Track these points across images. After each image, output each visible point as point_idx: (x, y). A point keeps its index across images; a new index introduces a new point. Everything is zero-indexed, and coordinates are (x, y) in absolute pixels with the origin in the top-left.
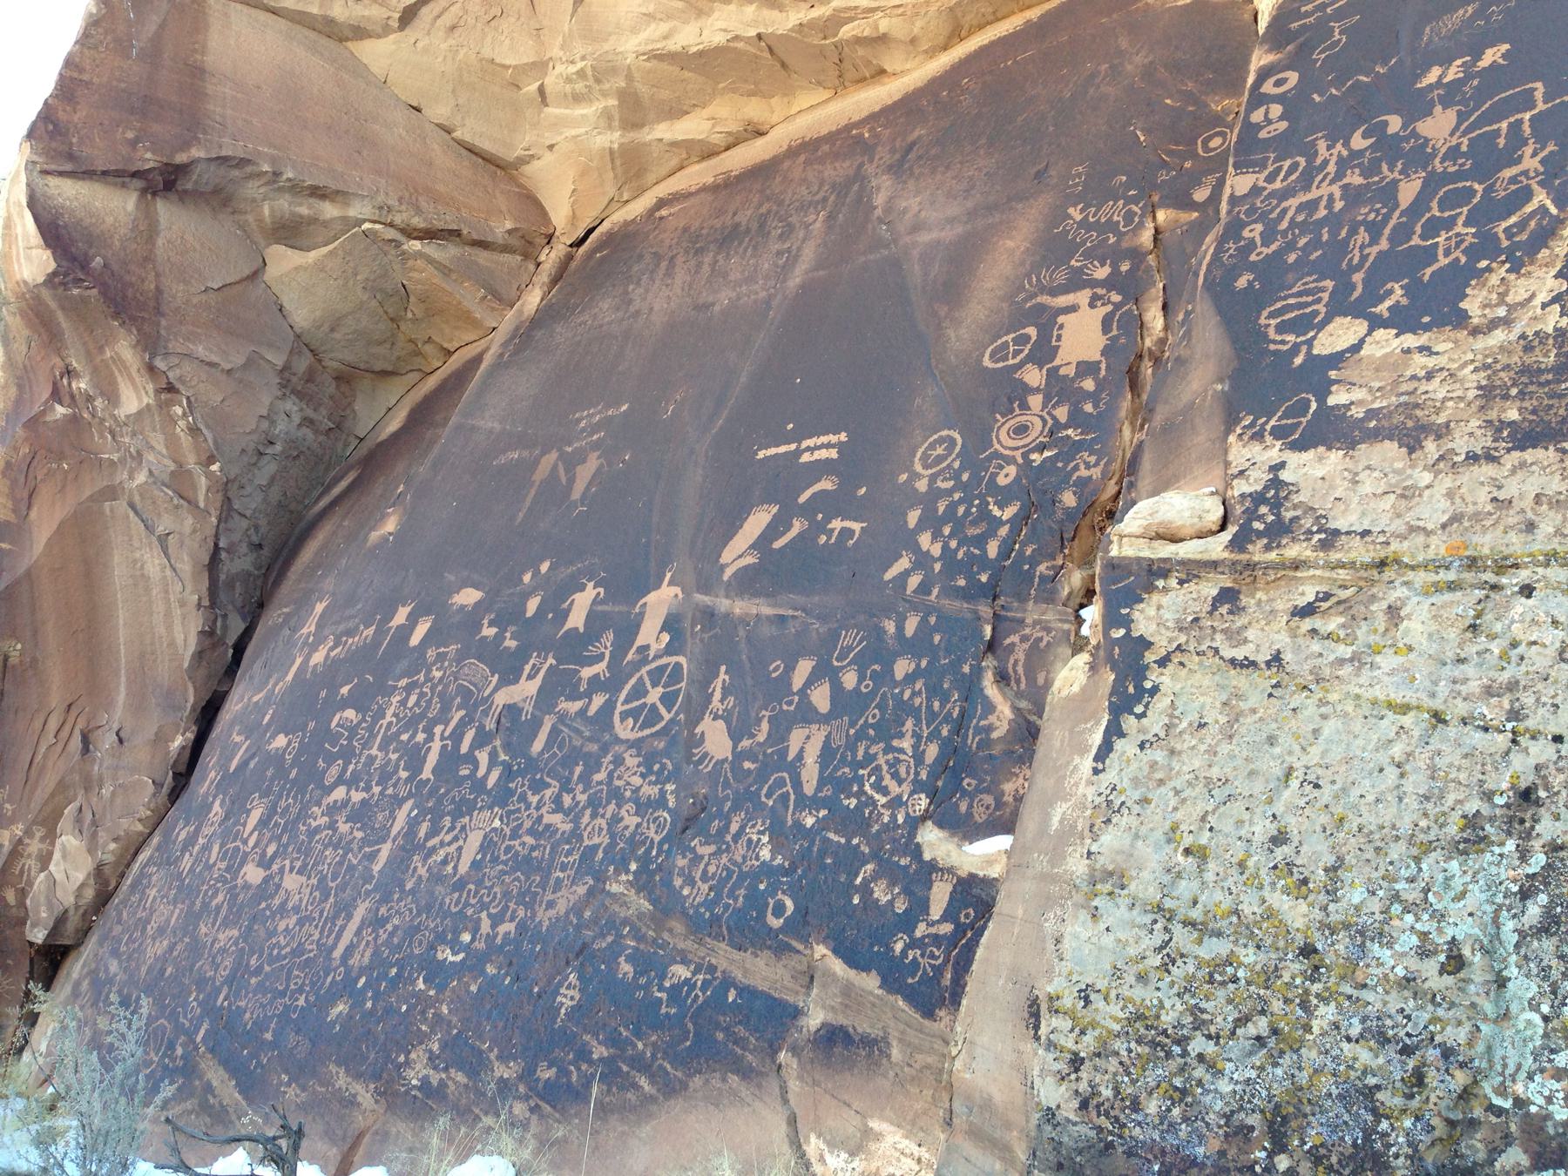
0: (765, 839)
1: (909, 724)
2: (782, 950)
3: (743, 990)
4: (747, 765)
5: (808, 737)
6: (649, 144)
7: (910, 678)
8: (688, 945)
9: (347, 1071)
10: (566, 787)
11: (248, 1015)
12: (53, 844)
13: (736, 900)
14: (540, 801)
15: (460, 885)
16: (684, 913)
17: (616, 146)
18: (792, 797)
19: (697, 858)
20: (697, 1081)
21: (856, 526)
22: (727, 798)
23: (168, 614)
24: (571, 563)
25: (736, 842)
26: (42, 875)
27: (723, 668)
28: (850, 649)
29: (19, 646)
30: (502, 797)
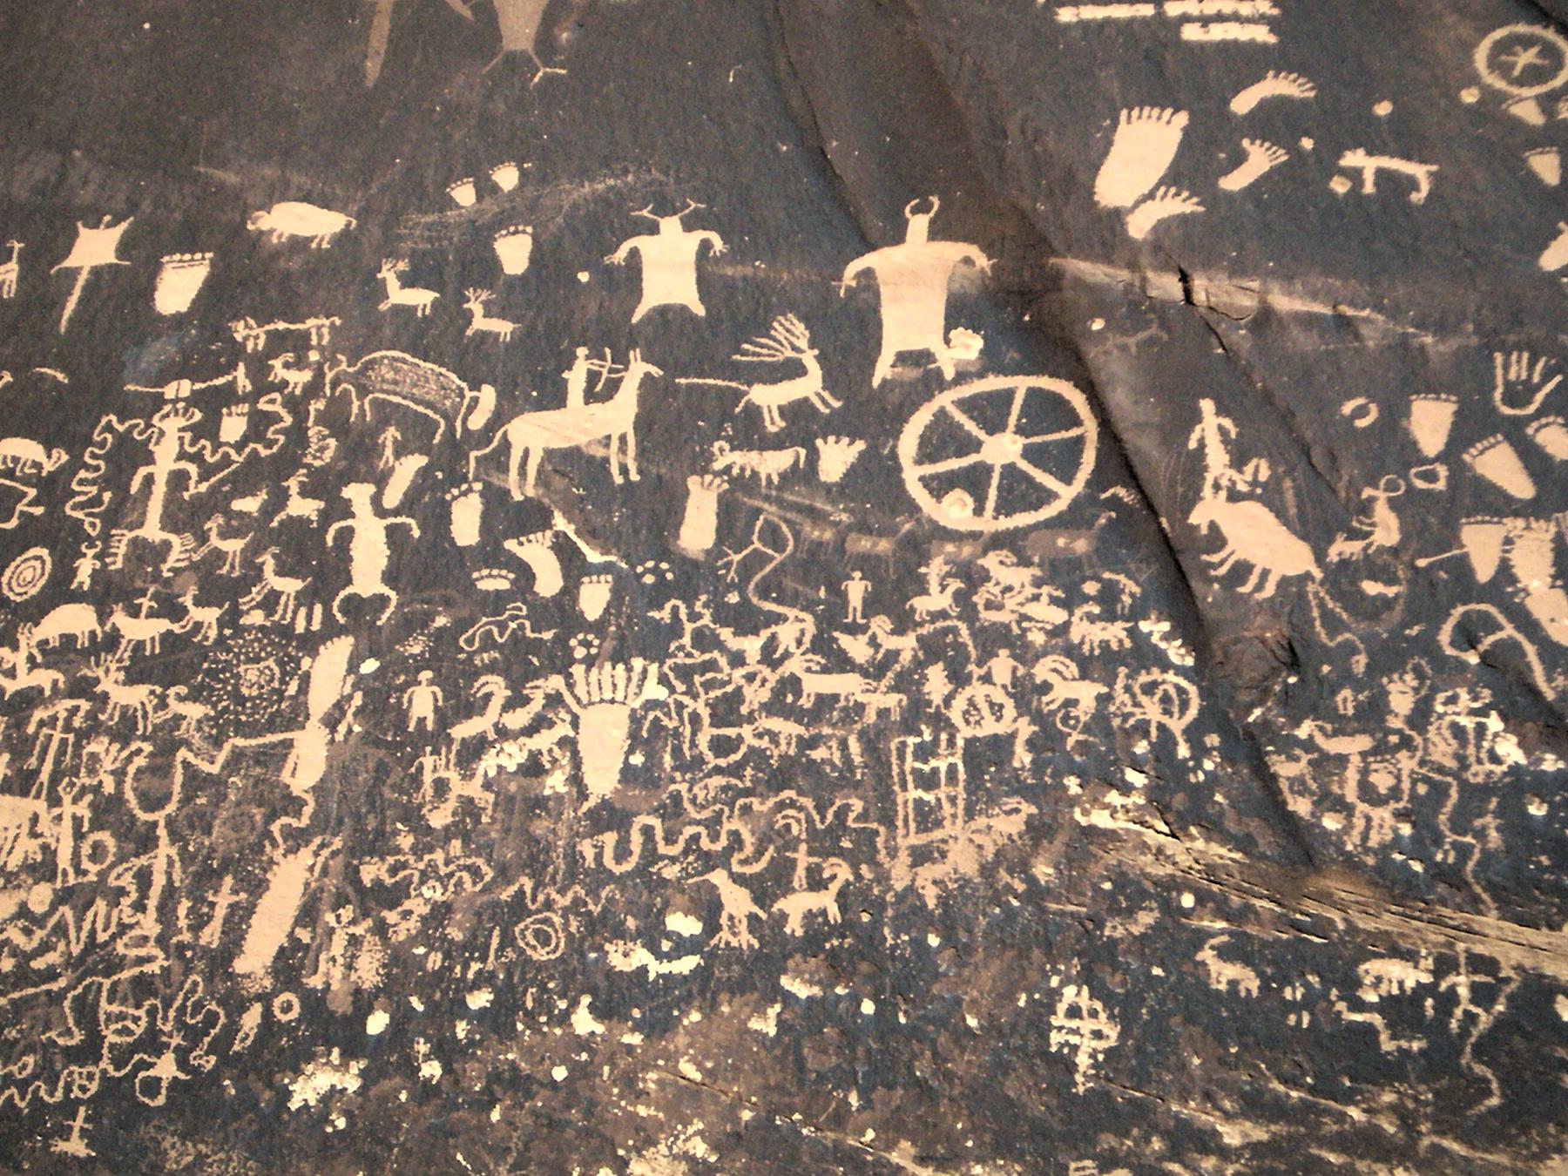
0: (1494, 723)
4: (1371, 588)
5: (1508, 541)
8: (1388, 922)
10: (832, 618)
13: (1481, 834)
14: (770, 646)
15: (610, 817)
16: (1351, 865)
18: (1530, 650)
21: (1419, 171)
22: (1350, 650)
24: (584, 174)
25: (1422, 731)
27: (1207, 406)
28: (1530, 389)
30: (634, 638)
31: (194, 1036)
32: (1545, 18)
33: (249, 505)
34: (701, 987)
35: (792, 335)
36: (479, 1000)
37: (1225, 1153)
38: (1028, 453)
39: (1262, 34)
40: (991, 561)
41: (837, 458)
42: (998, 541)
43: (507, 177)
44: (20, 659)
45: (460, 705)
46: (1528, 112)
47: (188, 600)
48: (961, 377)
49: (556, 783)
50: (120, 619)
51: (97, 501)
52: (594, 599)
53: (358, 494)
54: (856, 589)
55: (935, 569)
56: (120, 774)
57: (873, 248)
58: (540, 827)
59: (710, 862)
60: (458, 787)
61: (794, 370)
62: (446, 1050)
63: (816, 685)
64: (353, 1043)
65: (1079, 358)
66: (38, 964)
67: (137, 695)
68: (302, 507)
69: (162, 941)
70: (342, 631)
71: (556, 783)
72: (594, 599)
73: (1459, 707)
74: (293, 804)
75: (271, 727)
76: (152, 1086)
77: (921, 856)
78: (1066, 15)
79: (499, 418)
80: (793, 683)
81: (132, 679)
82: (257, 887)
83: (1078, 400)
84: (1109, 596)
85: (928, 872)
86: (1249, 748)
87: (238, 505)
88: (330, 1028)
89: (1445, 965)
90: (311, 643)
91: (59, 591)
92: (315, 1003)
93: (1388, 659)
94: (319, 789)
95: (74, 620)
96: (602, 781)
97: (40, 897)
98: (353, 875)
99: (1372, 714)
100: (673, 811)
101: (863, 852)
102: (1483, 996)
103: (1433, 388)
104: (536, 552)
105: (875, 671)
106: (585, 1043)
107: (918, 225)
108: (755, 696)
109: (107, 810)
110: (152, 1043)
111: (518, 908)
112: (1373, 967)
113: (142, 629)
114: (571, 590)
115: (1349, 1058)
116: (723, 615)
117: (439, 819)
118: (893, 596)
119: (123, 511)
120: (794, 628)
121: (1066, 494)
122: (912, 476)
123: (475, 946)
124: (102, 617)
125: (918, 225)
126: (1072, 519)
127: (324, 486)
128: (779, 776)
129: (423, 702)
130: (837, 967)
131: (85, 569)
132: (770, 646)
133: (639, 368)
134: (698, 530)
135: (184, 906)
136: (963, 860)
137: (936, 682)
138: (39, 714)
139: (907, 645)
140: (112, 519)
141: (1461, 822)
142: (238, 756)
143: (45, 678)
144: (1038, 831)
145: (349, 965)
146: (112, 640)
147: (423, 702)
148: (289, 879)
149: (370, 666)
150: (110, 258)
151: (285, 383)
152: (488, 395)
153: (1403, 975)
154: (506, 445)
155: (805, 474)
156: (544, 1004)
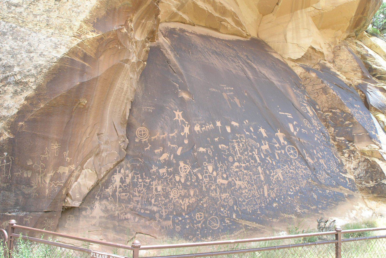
1: (331, 160)
2: (337, 187)
3: (336, 192)
6: (179, 15)
7: (327, 154)
9: (286, 214)
11: (248, 210)
12: (81, 172)
14: (286, 167)
15: (284, 182)
17: (175, 12)
19: (319, 177)
20: (339, 203)
23: (123, 101)
26: (76, 183)
29: (86, 102)
31: (264, 202)
32: (306, 119)
33: (246, 153)
34: (294, 195)
35: (274, 140)
36: (282, 197)
37: (325, 204)
38: (294, 152)
39: (291, 117)
40: (295, 161)
41: (283, 152)
42: (295, 159)
43: (247, 121)
44: (234, 167)
45: (271, 173)
46: (308, 127)
47: (245, 162)
48: (287, 145)
49: (279, 179)
50: (241, 164)
51: (233, 152)
52: (274, 163)
53: (254, 152)
54: (289, 163)
55: (293, 161)
56: (248, 179)
57: (276, 133)
58: (280, 183)
59: (291, 185)
60: (274, 180)
61: (276, 144)
62: (282, 201)
63: (291, 171)
64: (276, 202)
65: (295, 145)
66: (249, 197)
67: (245, 171)
68: (250, 154)
69: (258, 194)
70: (259, 166)
71: (279, 179)
72: (274, 163)
73: (324, 173)
74: (262, 181)
75: (258, 174)
76: (263, 206)
77: (302, 184)
78: (280, 113)
79: (260, 146)
80: (289, 171)
81: (245, 170)
82: (264, 189)
83: (295, 148)
84: (303, 164)
85: (303, 185)
86: (315, 175)
87: (245, 153)
88: (274, 201)
89: (330, 191)
90: (257, 167)
91: (234, 161)
92: (272, 198)
93: (320, 169)
94: (264, 180)
95: (236, 164)
96: (282, 179)
97: (247, 191)
98: (270, 188)
99: (320, 174)
100: (287, 181)
101: (299, 184)
102: (332, 192)
103: (314, 149)
104: (268, 158)
105: (293, 169)
106: (290, 200)
107: (279, 131)
108: (288, 172)
109: (248, 182)
110: (261, 203)
111: (281, 190)
112: (327, 191)
113: (243, 165)
114: (272, 162)
115: (327, 197)
116: (282, 164)
117: (274, 182)
118: (291, 164)
119: (236, 153)
120: (287, 166)
121: (297, 155)
122: (288, 153)
123: (280, 193)
124: (239, 164)
125: (279, 131)
126: (298, 158)
127: (251, 151)
128: (292, 178)
129: (268, 172)
130: (301, 193)
131: (236, 159)
132: (286, 167)
133: (267, 142)
134: (277, 158)
135: (259, 191)
136: (304, 184)
137: (297, 171)
138: (239, 173)
139: (294, 167)
140: (236, 154)
141: (327, 180)
142: (257, 177)
143: (237, 170)
144: (307, 182)
145: (273, 195)
146: (241, 166)
147: (268, 172)
148: (265, 187)
149: (262, 169)
150: (221, 125)
151: (243, 141)
152: (258, 143)
153: (328, 191)
154: (262, 149)
155: (281, 153)
156: (287, 197)
